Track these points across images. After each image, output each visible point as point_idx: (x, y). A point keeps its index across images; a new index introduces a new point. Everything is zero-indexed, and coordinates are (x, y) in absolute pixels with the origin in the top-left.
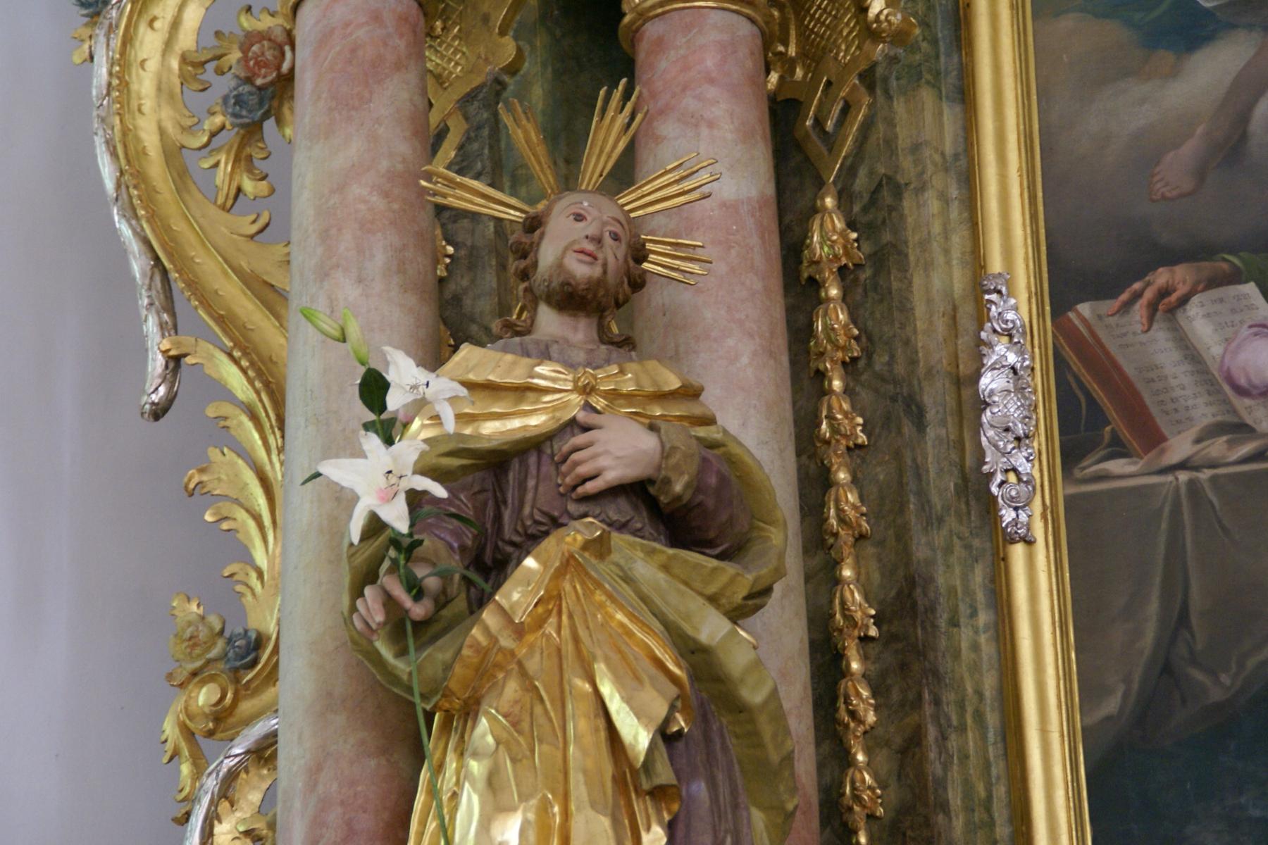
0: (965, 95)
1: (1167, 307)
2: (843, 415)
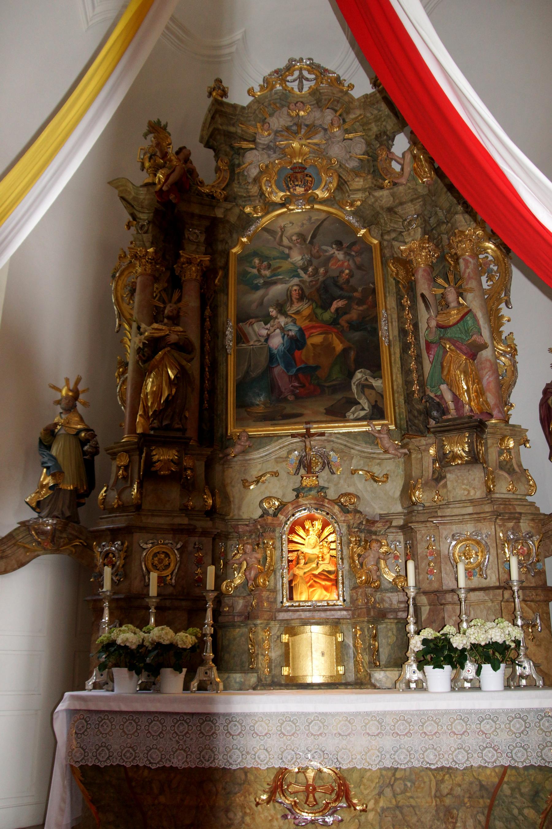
0: (227, 294)
1: (251, 324)
2: (208, 336)
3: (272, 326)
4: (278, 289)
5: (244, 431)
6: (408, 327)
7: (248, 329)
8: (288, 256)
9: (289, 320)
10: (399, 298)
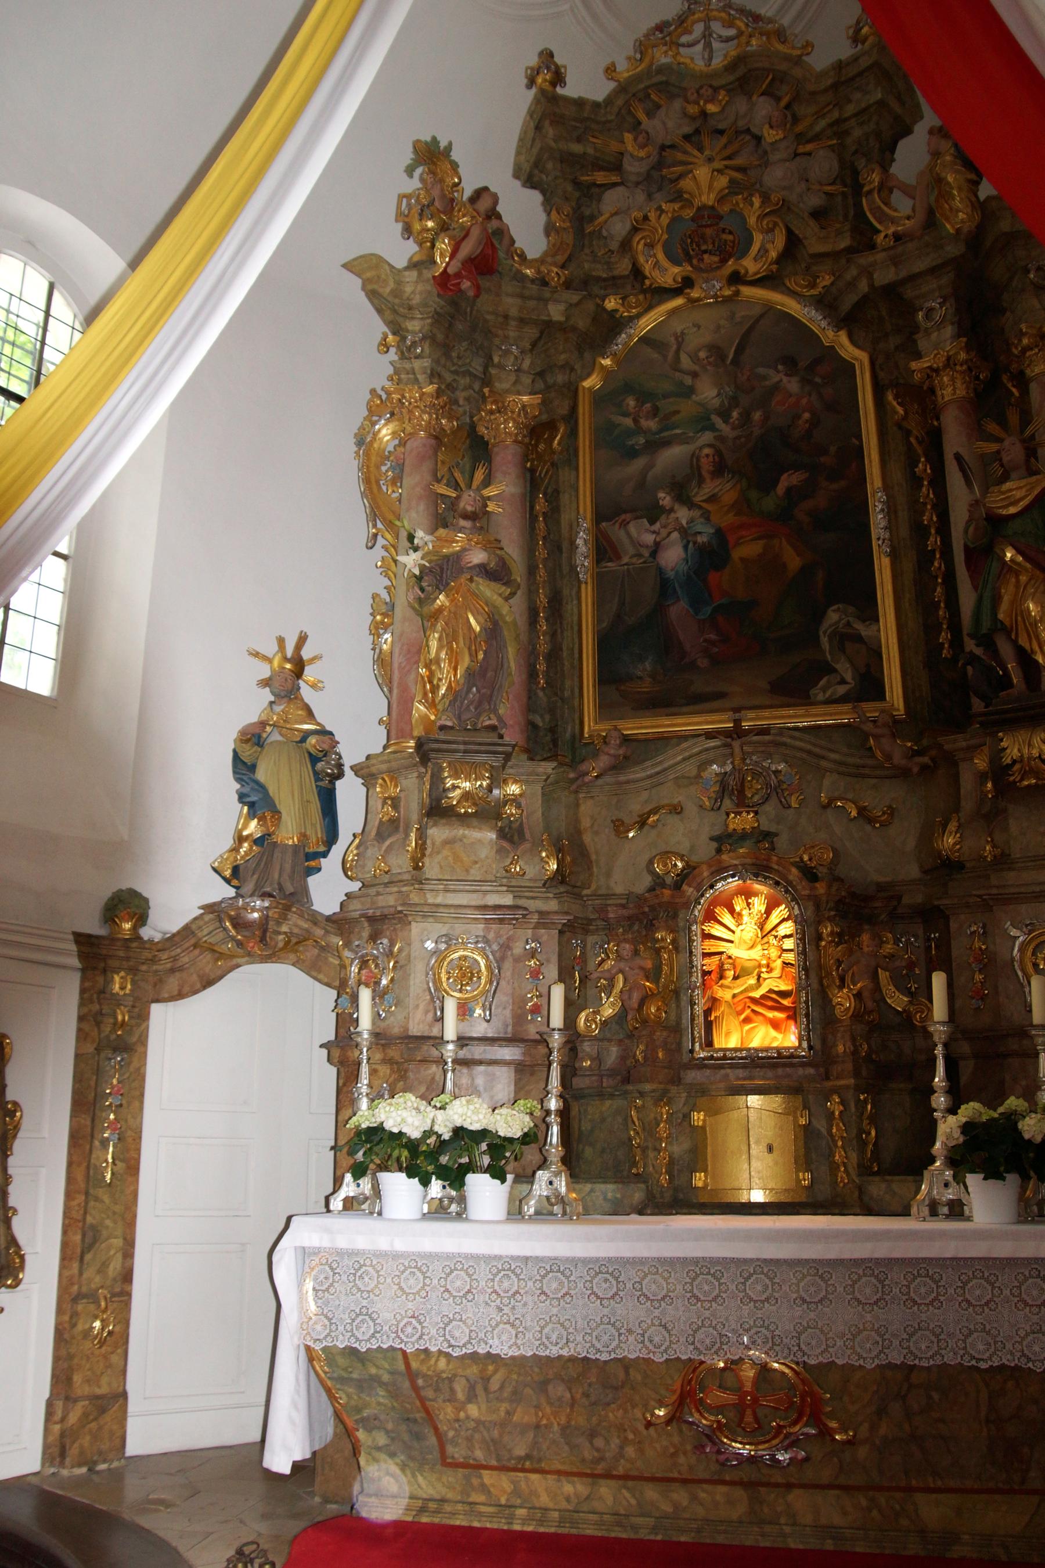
0: (577, 469)
1: (624, 524)
3: (665, 527)
4: (673, 455)
5: (616, 728)
6: (929, 517)
8: (691, 391)
9: (696, 513)
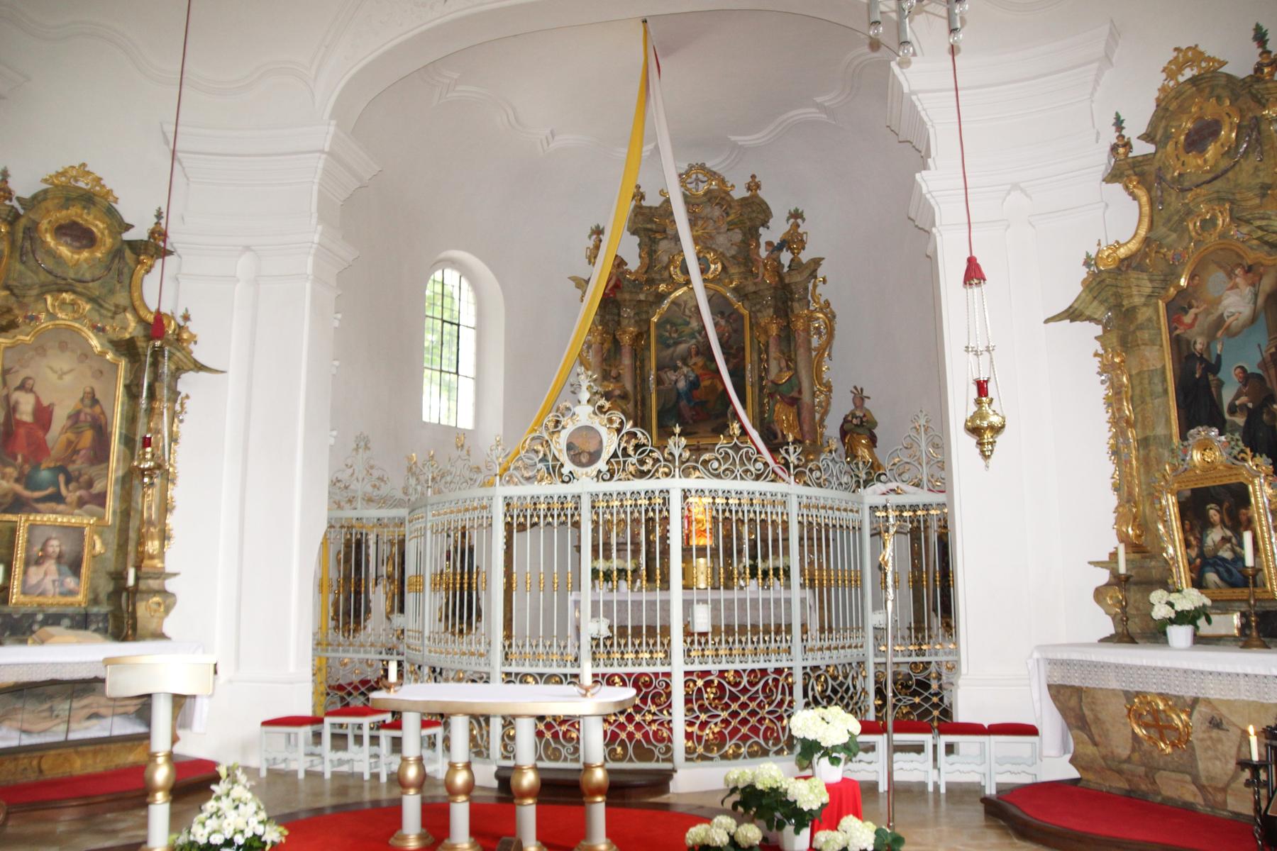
4: (683, 347)
7: (664, 376)
8: (688, 323)
10: (760, 353)
